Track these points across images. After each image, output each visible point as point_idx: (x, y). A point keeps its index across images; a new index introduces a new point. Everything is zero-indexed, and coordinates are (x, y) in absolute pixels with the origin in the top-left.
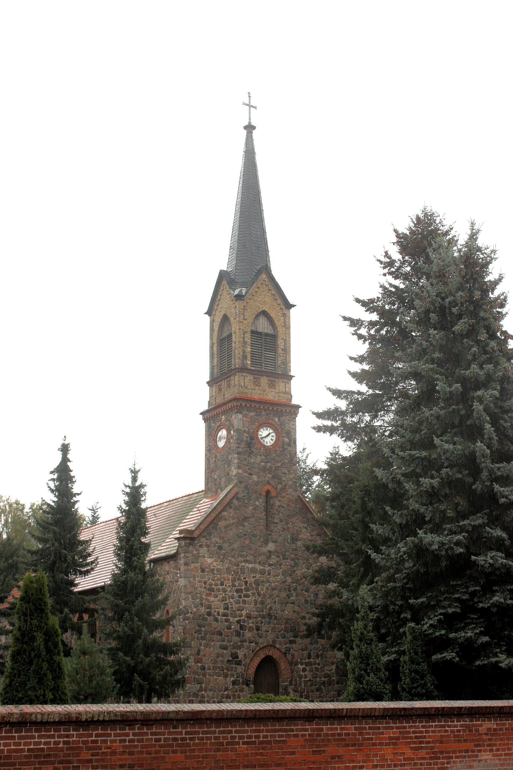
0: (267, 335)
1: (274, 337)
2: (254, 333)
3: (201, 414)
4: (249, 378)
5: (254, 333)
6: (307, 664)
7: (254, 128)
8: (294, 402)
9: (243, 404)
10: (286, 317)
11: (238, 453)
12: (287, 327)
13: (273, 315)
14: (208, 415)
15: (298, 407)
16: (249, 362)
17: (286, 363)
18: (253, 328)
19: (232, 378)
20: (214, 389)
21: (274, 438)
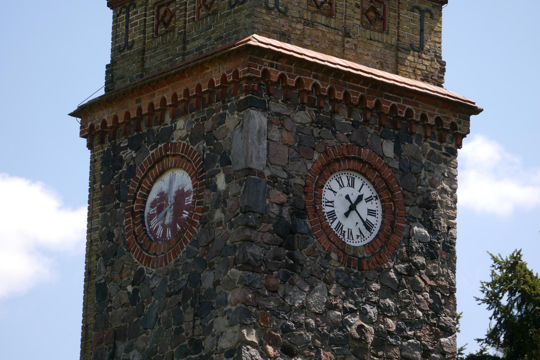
8: (454, 87)
9: (275, 75)
11: (248, 265)
15: (466, 110)
21: (376, 221)
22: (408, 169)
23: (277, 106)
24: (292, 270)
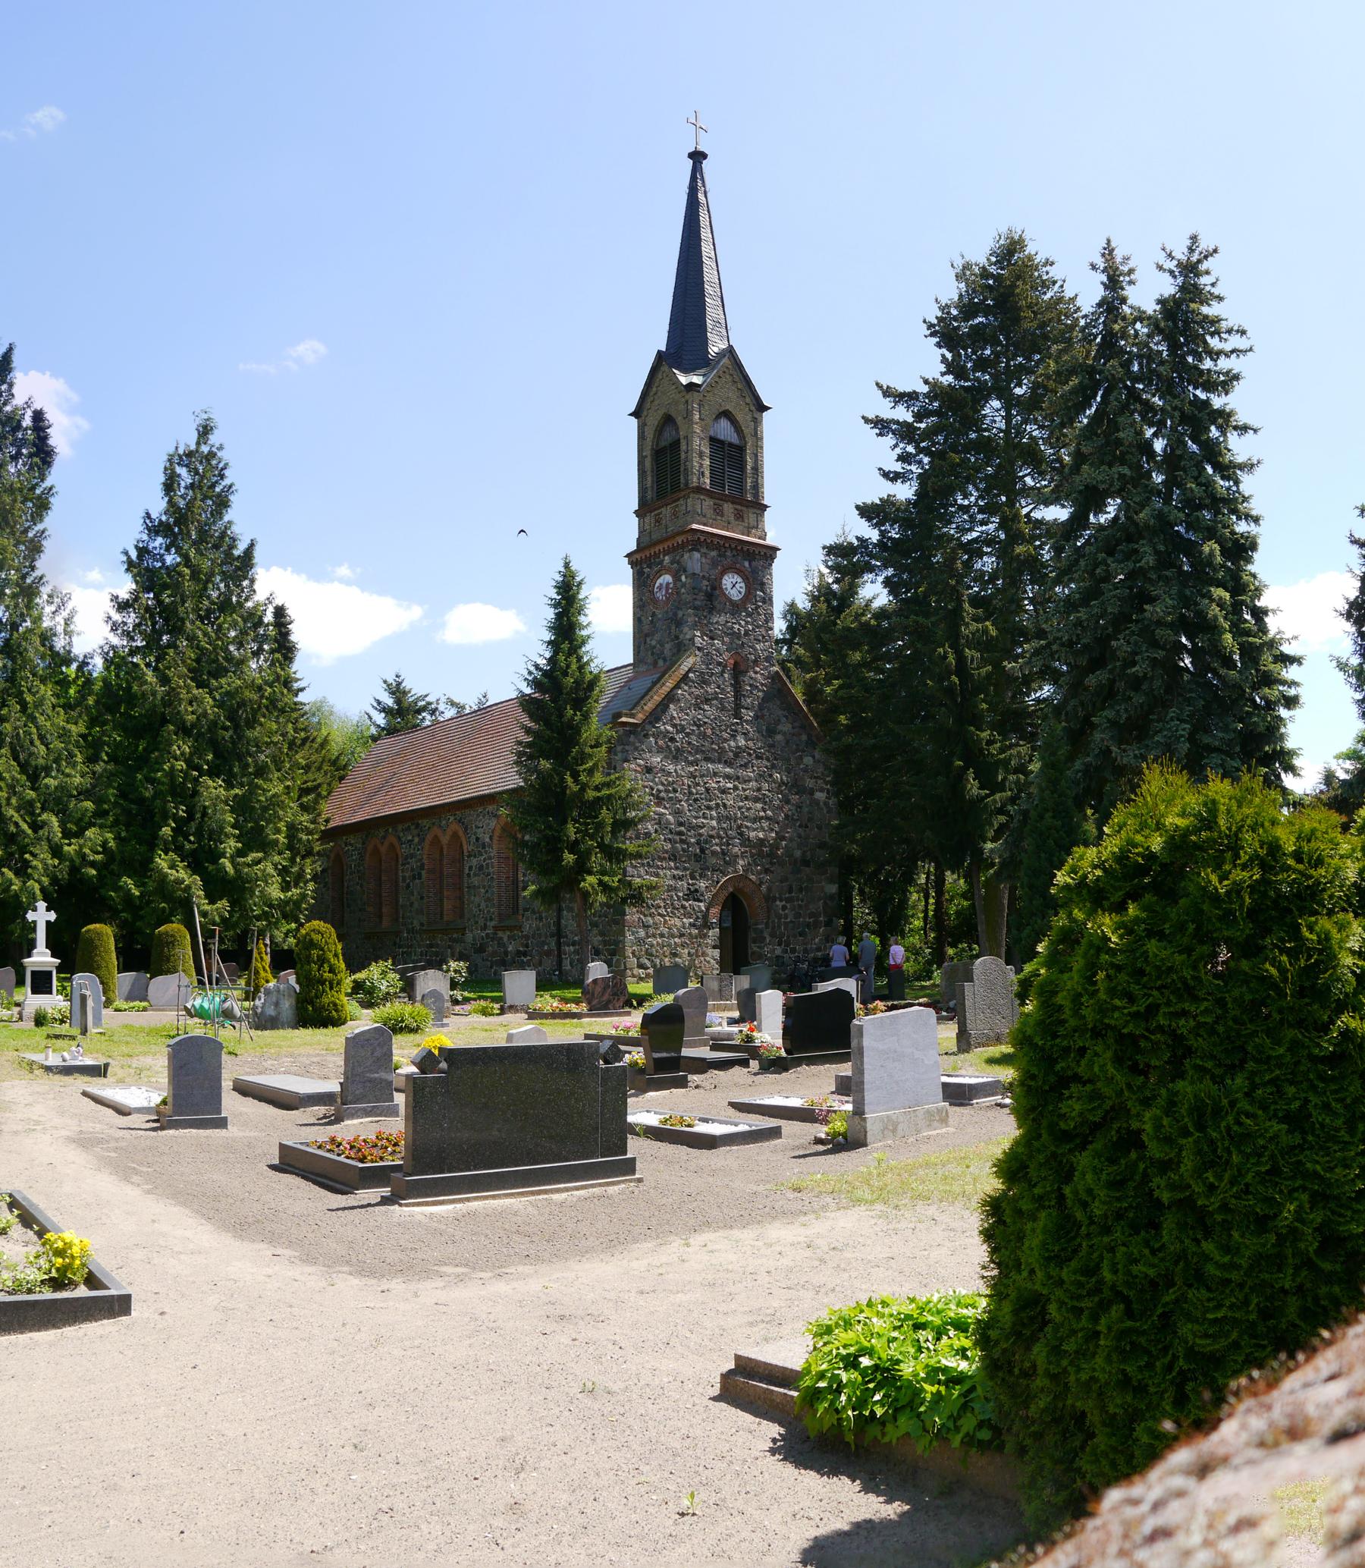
0: (731, 445)
1: (741, 449)
2: (714, 441)
3: (627, 556)
4: (708, 503)
5: (714, 441)
6: (788, 900)
7: (704, 156)
8: (770, 541)
10: (757, 422)
11: (695, 608)
12: (758, 438)
13: (739, 417)
14: (638, 556)
16: (708, 481)
17: (757, 488)
18: (712, 433)
19: (681, 502)
20: (647, 520)
21: (743, 591)
22: (754, 571)
23: (704, 550)
24: (712, 610)
